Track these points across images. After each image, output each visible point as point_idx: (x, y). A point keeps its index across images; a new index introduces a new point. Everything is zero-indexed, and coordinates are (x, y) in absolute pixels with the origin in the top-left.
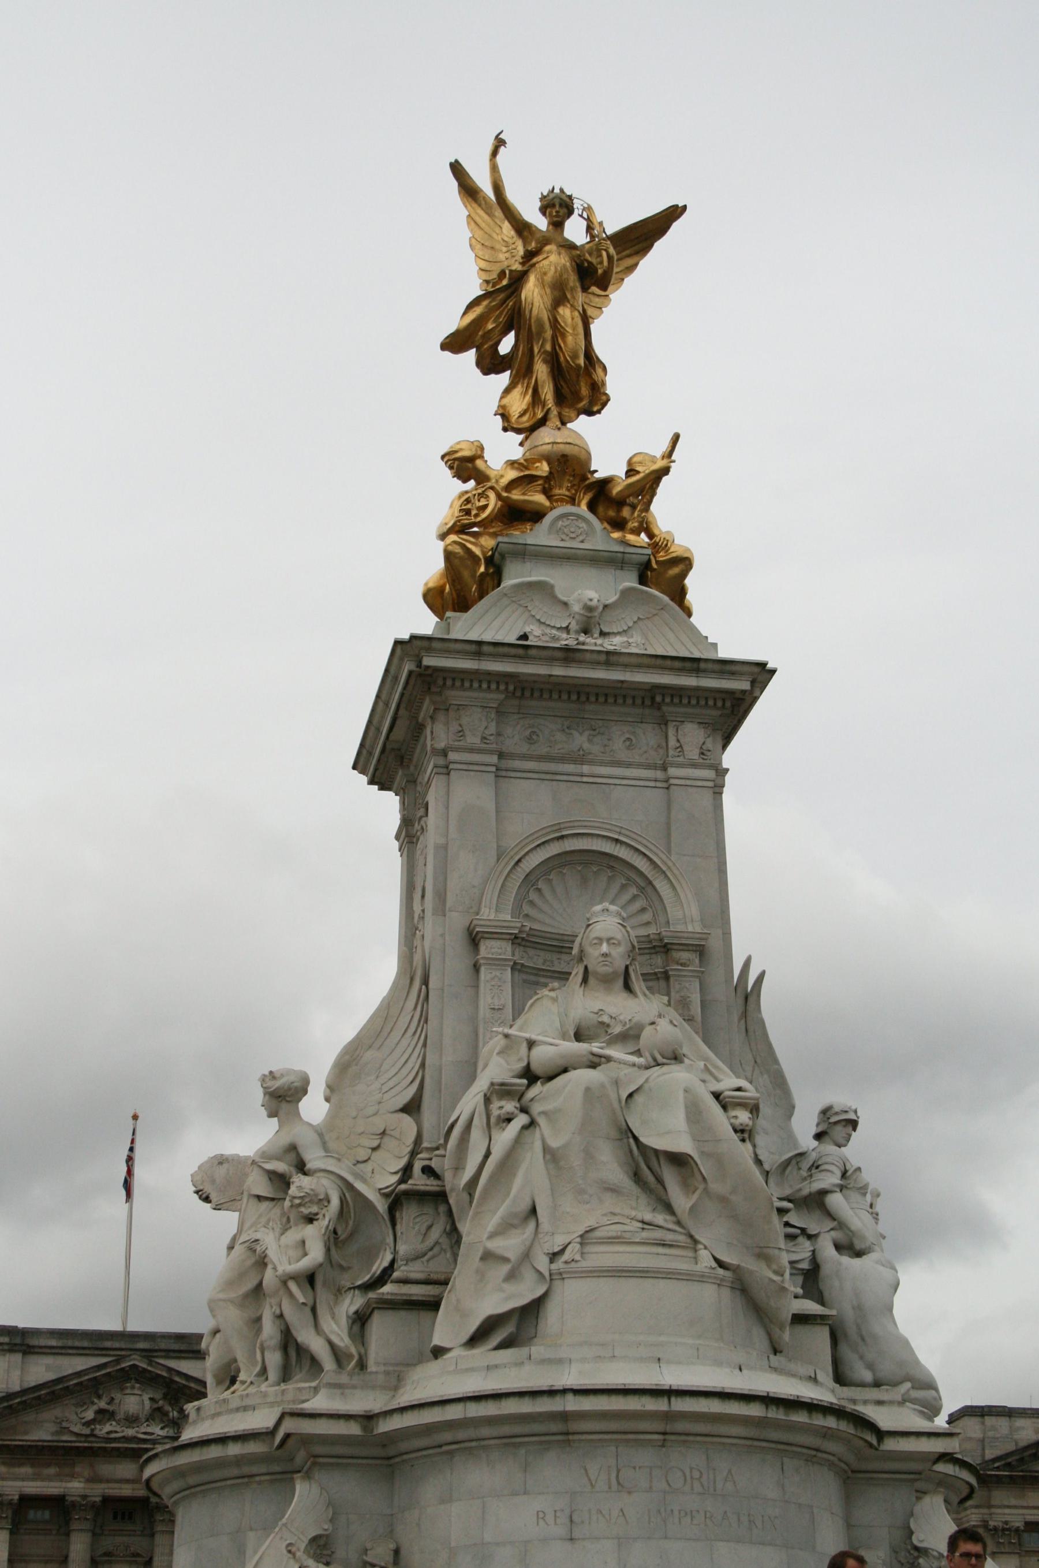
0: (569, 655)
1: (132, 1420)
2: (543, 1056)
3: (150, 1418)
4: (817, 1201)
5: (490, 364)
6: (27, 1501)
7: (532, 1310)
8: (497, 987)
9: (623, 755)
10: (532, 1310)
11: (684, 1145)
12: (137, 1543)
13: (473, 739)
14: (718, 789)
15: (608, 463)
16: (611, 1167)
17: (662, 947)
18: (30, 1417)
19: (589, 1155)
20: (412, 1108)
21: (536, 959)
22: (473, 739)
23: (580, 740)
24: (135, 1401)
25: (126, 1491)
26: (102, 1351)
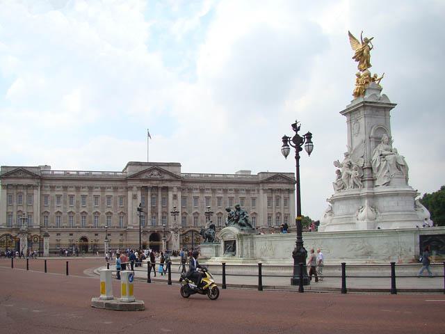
6: (143, 187)
8: (373, 144)
11: (403, 164)
20: (362, 157)
24: (156, 173)
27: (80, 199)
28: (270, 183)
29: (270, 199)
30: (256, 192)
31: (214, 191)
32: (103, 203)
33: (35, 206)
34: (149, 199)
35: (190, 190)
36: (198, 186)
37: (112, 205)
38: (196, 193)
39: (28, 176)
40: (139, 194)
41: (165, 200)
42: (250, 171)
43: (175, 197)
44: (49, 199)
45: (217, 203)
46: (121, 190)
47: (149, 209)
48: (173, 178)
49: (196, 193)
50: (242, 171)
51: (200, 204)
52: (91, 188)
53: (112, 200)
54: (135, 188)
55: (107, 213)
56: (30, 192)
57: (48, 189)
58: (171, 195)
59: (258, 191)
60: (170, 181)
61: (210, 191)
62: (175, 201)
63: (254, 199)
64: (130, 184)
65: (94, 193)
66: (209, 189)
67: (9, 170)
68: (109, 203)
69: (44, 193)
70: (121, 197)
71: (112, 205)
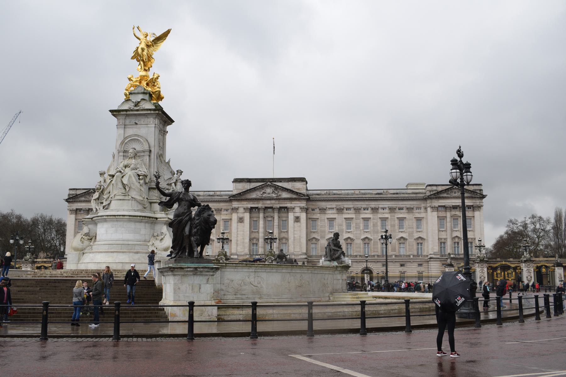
0: (132, 110)
1: (269, 194)
3: (272, 193)
4: (170, 184)
5: (138, 61)
6: (252, 208)
10: (109, 204)
12: (272, 214)
13: (121, 123)
16: (120, 185)
18: (252, 194)
19: (117, 184)
22: (121, 123)
24: (269, 190)
25: (269, 206)
26: (263, 182)
29: (441, 219)
30: (423, 210)
31: (357, 210)
34: (261, 223)
36: (334, 205)
38: (331, 214)
40: (247, 216)
41: (284, 225)
43: (297, 219)
46: (225, 212)
47: (261, 235)
48: (294, 196)
54: (241, 210)
58: (291, 216)
59: (426, 208)
60: (291, 199)
61: (352, 211)
62: (297, 224)
63: (419, 220)
64: (235, 204)
67: (79, 192)
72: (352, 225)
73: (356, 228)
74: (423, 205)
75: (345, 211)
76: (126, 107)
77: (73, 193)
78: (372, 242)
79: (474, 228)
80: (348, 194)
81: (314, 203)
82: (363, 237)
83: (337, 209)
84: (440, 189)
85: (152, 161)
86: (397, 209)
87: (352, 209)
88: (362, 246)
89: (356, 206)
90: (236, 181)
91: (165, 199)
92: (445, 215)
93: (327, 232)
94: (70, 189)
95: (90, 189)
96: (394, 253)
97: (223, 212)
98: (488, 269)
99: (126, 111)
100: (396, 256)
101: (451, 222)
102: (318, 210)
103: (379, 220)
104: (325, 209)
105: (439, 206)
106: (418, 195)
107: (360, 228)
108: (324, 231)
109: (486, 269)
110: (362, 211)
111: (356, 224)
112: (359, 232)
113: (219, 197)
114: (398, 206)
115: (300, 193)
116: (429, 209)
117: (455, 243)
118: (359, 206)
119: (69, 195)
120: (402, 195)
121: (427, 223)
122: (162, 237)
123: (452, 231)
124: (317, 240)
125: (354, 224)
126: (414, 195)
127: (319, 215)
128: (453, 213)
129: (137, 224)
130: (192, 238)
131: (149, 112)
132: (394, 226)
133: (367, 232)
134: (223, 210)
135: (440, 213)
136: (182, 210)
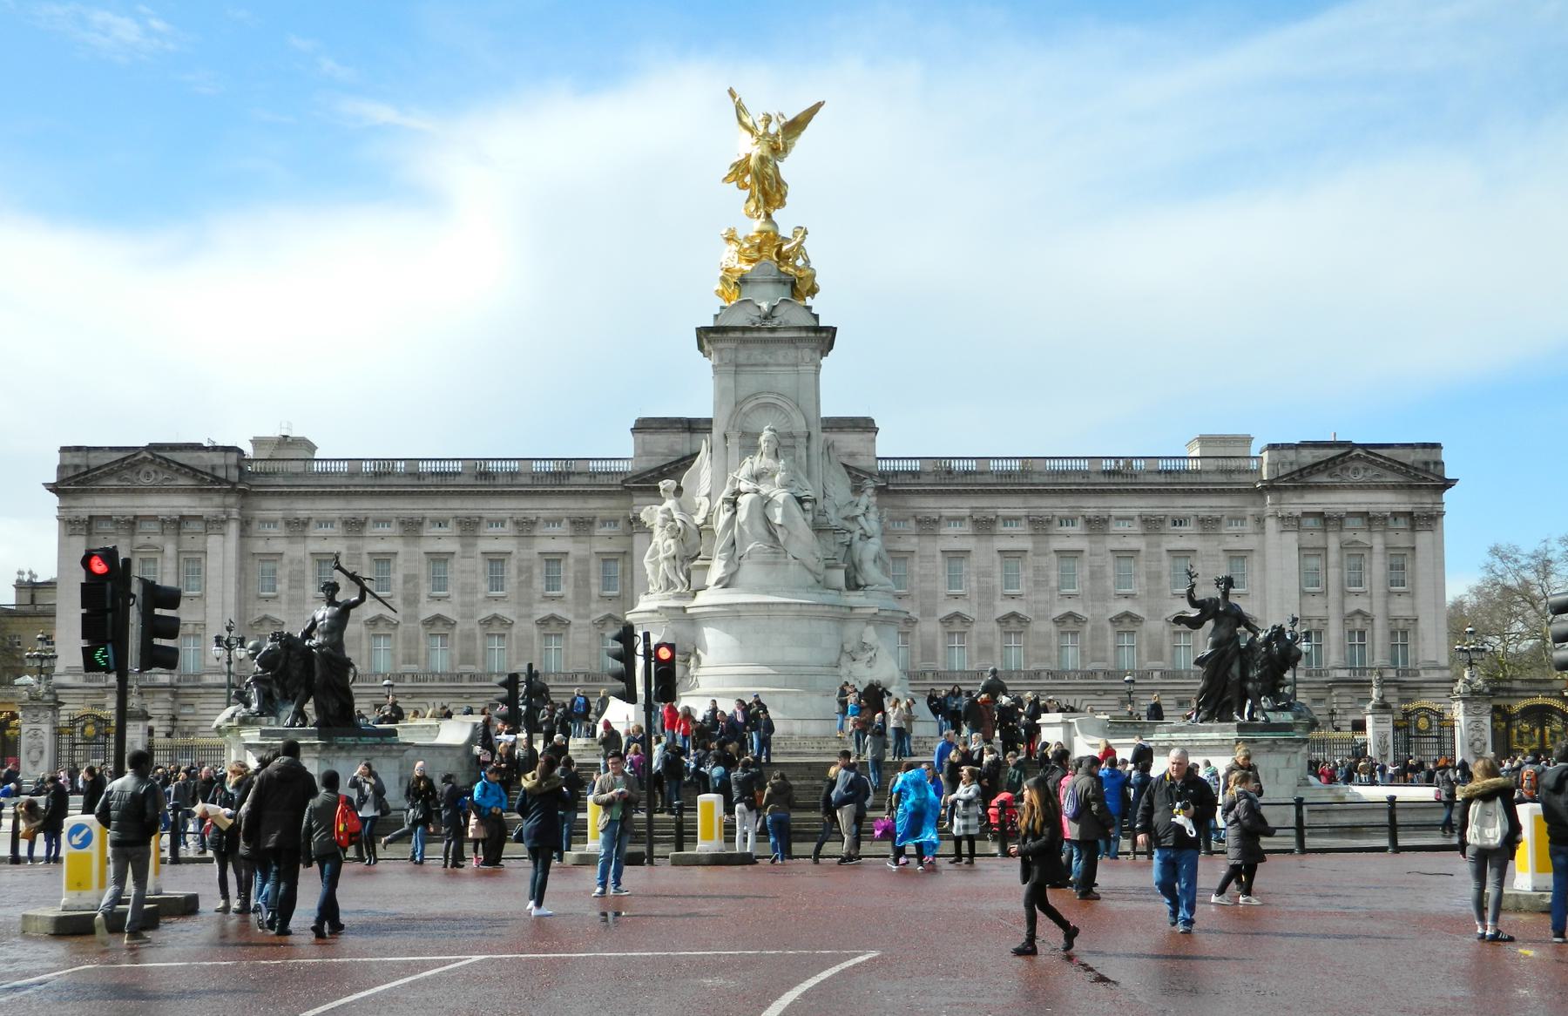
2: (743, 486)
4: (854, 519)
5: (745, 186)
7: (733, 575)
9: (782, 361)
14: (817, 373)
15: (785, 231)
16: (760, 528)
17: (791, 436)
19: (751, 526)
20: (708, 495)
21: (748, 441)
23: (766, 358)
27: (423, 570)
28: (1320, 488)
30: (1250, 526)
31: (1040, 525)
32: (527, 583)
33: (213, 598)
35: (929, 525)
36: (963, 506)
37: (566, 590)
38: (955, 537)
39: (183, 481)
42: (1247, 440)
44: (283, 572)
45: (1054, 574)
46: (606, 530)
49: (955, 537)
50: (1204, 440)
51: (971, 584)
52: (469, 527)
53: (568, 571)
55: (544, 622)
56: (188, 543)
57: (280, 530)
59: (1260, 520)
65: (485, 545)
66: (1017, 519)
67: (96, 460)
68: (552, 581)
69: (259, 546)
70: (607, 559)
71: (566, 590)
72: (1023, 574)
73: (1036, 583)
74: (1251, 510)
75: (1000, 528)
76: (739, 319)
77: (77, 461)
78: (1088, 627)
79: (1413, 585)
80: (1010, 474)
81: (897, 501)
82: (1058, 612)
83: (976, 522)
84: (1308, 457)
85: (814, 459)
86: (1169, 523)
87: (1024, 522)
88: (1054, 641)
89: (1033, 512)
90: (644, 426)
91: (1195, 613)
92: (1321, 543)
93: (941, 596)
94: (64, 450)
95: (136, 450)
96: (1159, 664)
97: (600, 531)
98: (1493, 720)
99: (744, 329)
100: (1164, 674)
101: (1341, 566)
102: (912, 523)
103: (1110, 558)
104: (935, 522)
105: (1305, 514)
106: (1236, 478)
107: (1047, 581)
108: (934, 594)
109: (1487, 720)
110: (1056, 528)
111: (1037, 569)
112: (1044, 597)
113: (585, 480)
114: (1172, 512)
115: (857, 470)
116: (1271, 524)
117: (1352, 632)
118: (1046, 512)
119: (61, 468)
120: (1184, 478)
121: (1264, 569)
122: (871, 654)
123: (1344, 593)
124: (910, 621)
125: (1030, 573)
126: (1223, 479)
127: (915, 540)
128: (1348, 536)
129: (814, 623)
130: (1250, 686)
131: (804, 334)
132: (1159, 576)
133: (1070, 596)
134: (597, 524)
135: (1307, 535)
136: (1224, 632)
